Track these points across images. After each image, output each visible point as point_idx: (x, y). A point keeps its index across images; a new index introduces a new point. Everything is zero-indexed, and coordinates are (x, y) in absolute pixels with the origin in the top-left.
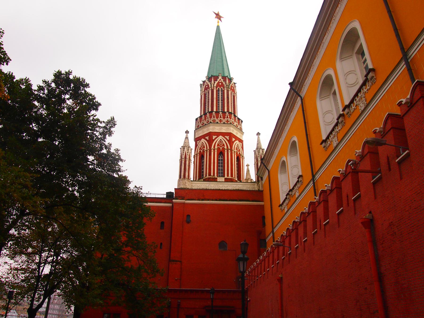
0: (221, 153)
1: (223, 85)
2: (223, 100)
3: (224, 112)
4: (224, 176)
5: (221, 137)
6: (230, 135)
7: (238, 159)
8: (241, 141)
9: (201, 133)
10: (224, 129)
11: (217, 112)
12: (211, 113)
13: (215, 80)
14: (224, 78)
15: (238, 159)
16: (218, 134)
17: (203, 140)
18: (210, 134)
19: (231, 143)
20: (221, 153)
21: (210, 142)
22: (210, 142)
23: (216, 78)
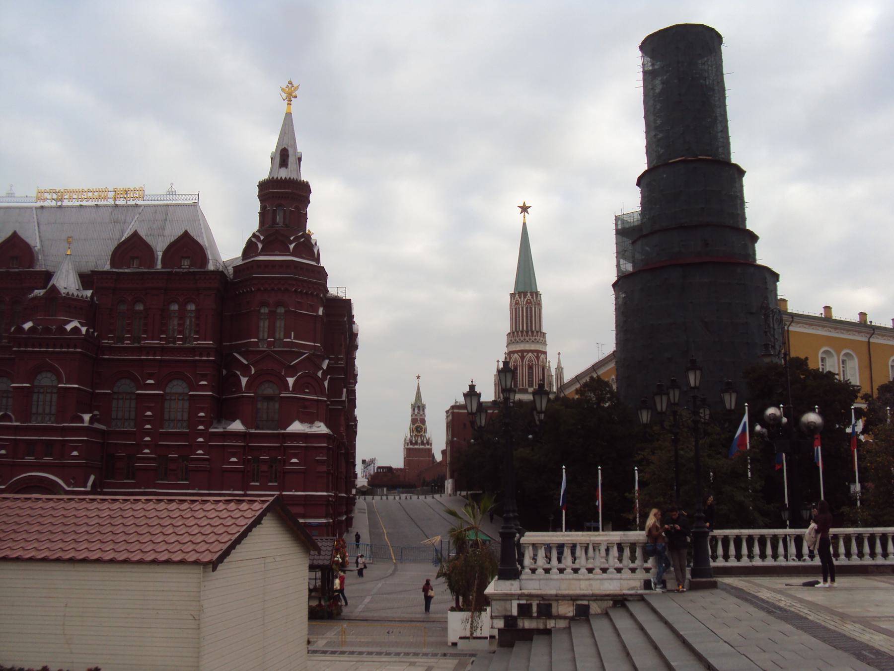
0: (530, 368)
1: (531, 302)
2: (531, 317)
3: (532, 332)
4: (532, 386)
5: (530, 354)
6: (538, 352)
7: (543, 370)
8: (545, 353)
9: (514, 348)
10: (533, 347)
11: (527, 332)
12: (522, 332)
13: (525, 297)
14: (532, 294)
15: (543, 370)
16: (528, 351)
17: (516, 355)
18: (522, 351)
19: (538, 358)
20: (530, 368)
21: (522, 358)
22: (522, 358)
23: (525, 294)
